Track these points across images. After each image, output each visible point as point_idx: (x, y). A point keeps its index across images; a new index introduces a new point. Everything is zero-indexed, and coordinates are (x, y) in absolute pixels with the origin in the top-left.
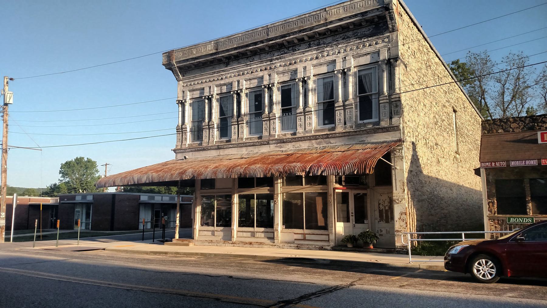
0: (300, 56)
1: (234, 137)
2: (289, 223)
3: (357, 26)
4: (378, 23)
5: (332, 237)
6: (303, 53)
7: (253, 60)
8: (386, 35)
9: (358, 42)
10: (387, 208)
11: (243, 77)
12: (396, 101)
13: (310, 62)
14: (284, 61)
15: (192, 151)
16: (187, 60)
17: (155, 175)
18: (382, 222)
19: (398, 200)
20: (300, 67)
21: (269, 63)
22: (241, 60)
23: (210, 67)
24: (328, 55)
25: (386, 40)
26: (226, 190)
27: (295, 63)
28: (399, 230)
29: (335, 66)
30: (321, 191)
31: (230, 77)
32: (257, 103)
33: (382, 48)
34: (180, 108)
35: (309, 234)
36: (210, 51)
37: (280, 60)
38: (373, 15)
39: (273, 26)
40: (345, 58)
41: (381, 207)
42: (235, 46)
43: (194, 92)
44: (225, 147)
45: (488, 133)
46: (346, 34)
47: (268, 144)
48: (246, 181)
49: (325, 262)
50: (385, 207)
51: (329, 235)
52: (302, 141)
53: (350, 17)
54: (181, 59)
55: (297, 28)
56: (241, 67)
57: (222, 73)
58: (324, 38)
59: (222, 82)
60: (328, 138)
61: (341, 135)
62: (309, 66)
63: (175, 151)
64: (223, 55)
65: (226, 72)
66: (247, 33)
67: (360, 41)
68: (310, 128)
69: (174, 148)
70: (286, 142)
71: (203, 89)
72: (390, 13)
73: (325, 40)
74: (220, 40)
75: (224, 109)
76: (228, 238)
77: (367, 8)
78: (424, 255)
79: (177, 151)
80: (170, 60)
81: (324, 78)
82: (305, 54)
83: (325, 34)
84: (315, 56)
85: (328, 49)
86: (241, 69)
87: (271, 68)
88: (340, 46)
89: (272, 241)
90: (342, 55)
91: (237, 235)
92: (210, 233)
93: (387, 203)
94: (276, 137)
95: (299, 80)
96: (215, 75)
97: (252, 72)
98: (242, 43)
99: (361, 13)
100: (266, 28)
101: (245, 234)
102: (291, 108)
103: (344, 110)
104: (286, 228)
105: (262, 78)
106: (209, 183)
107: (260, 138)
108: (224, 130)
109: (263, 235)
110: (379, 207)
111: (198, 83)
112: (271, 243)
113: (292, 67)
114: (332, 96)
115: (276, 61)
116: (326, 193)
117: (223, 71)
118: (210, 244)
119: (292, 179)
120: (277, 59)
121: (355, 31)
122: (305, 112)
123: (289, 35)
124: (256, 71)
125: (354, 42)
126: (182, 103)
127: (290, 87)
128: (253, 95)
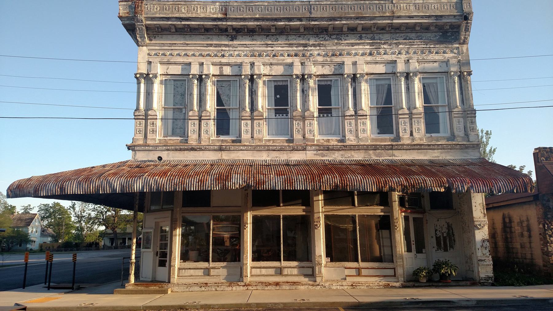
0: (347, 47)
1: (245, 136)
2: (336, 253)
3: (426, 28)
4: (451, 29)
5: (400, 271)
6: (353, 45)
7: (277, 40)
8: (455, 46)
9: (423, 46)
10: (445, 235)
11: (258, 59)
12: (471, 117)
13: (361, 57)
14: (324, 51)
15: (168, 150)
16: (168, 19)
17: (163, 181)
18: (440, 251)
19: (480, 225)
20: (348, 61)
21: (301, 48)
22: (255, 37)
23: (202, 37)
24: (385, 54)
25: (455, 51)
26: (233, 208)
27: (340, 55)
28: (483, 259)
29: (395, 67)
30: (382, 214)
31: (239, 55)
32: (278, 96)
33: (452, 58)
34: (142, 86)
35: (368, 268)
36: (213, 14)
37: (318, 48)
38: (448, 21)
39: (317, 3)
40: (408, 60)
41: (438, 233)
42: (257, 16)
43: (170, 66)
44: (233, 148)
45: (546, 160)
46: (409, 35)
47: (304, 149)
48: (263, 197)
49: (469, 304)
50: (443, 234)
51: (394, 269)
52: (354, 150)
53: (422, 17)
54: (158, 15)
55: (354, 13)
56: (257, 44)
57: (224, 48)
58: (380, 33)
59: (224, 60)
60: (392, 149)
61: (409, 147)
62: (361, 60)
63: (129, 148)
64: (234, 23)
65: (231, 48)
66: (278, 4)
67: (425, 46)
68: (365, 135)
69: (130, 143)
70: (332, 150)
71: (190, 64)
72: (467, 23)
73: (381, 36)
74: (231, 4)
75: (223, 98)
76: (237, 277)
77: (443, 12)
78: (520, 285)
79: (136, 148)
80: (136, 13)
81: (376, 79)
82: (355, 47)
83: (383, 29)
84: (368, 51)
85: (385, 46)
86: (256, 48)
87: (304, 55)
88: (401, 46)
89: (312, 279)
90: (403, 57)
91: (251, 272)
92: (200, 272)
93: (445, 230)
94: (315, 142)
95: (348, 76)
96: (211, 48)
97: (274, 56)
98: (269, 15)
99: (436, 16)
100: (307, 3)
101: (264, 271)
102: (331, 108)
103: (411, 119)
104: (331, 261)
105: (291, 65)
106: (199, 199)
107: (342, 141)
108: (223, 124)
109: (295, 271)
110: (436, 234)
111: (179, 55)
112: (311, 283)
113: (338, 59)
114: (388, 99)
115: (312, 48)
116: (389, 216)
117: (226, 46)
118: (203, 289)
119: (335, 196)
120: (314, 45)
121: (419, 34)
122: (304, 118)
123: (341, 18)
124: (282, 55)
125: (418, 45)
126: (148, 78)
127: (329, 83)
128: (273, 85)
